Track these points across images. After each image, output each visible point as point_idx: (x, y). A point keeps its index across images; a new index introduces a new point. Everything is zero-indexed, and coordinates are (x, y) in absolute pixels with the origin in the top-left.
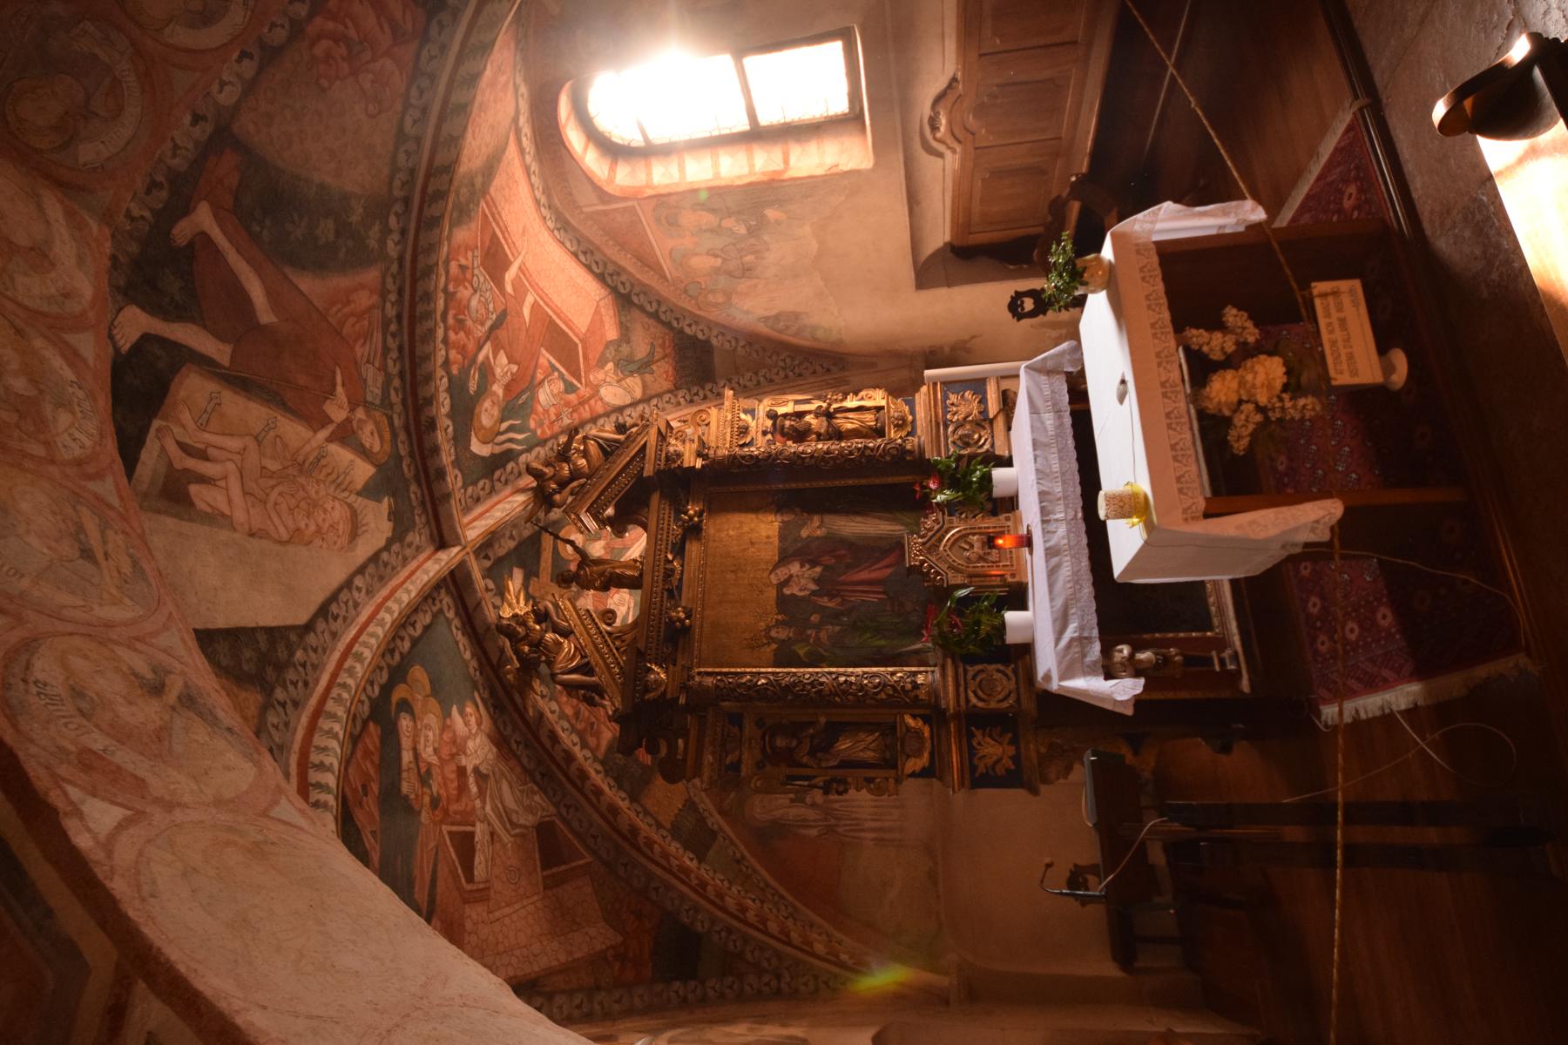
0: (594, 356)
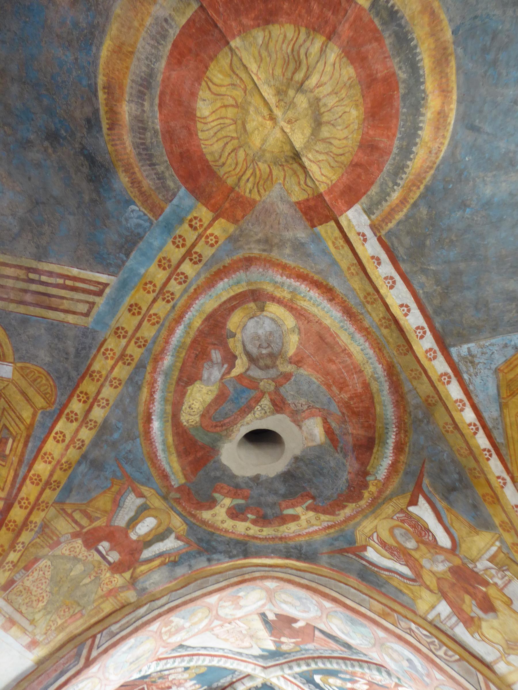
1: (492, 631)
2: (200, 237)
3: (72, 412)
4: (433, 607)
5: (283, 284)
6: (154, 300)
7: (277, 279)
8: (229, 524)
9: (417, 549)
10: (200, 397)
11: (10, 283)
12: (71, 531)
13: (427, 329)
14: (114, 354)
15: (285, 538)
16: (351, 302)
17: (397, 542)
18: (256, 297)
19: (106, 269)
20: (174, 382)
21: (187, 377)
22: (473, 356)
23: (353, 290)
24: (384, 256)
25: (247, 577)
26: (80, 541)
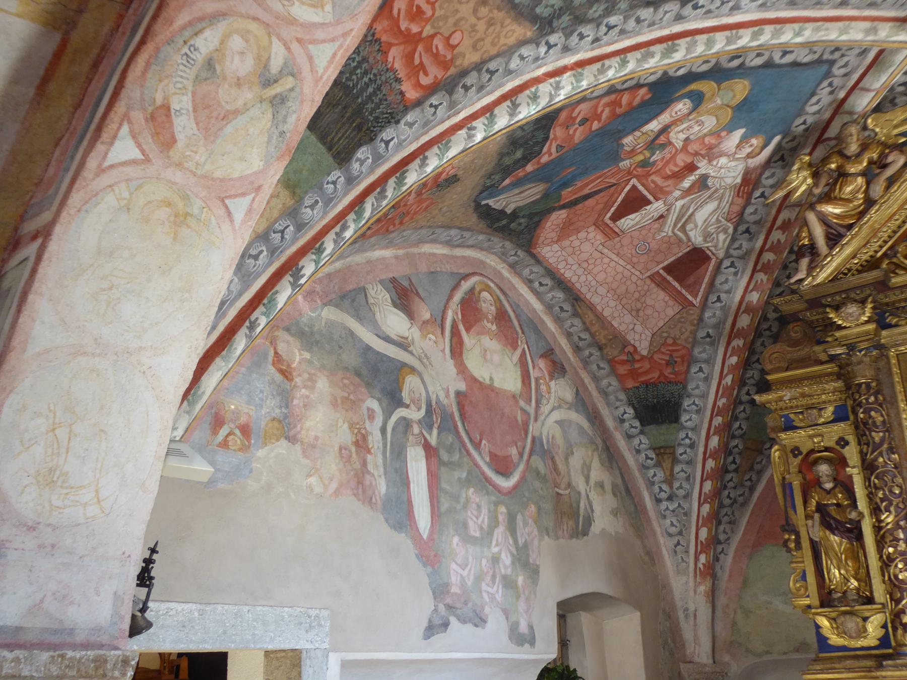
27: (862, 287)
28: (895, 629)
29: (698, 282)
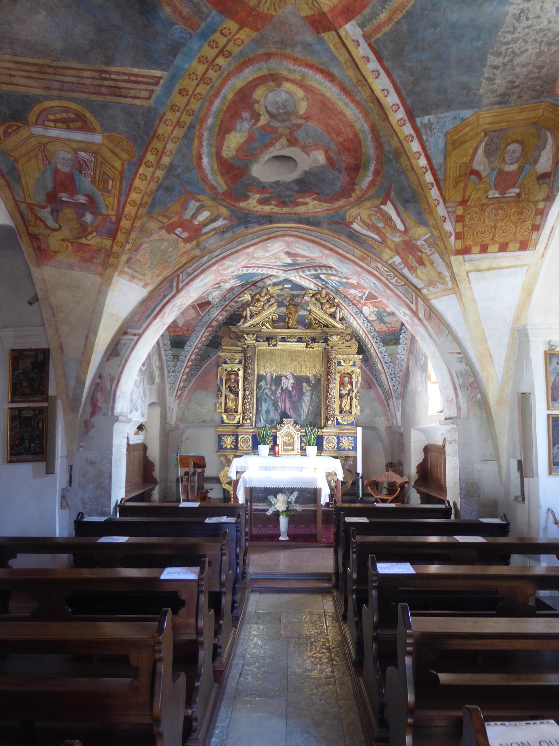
0: (377, 304)
1: (422, 274)
2: (229, 41)
3: (148, 161)
4: (392, 258)
5: (295, 71)
6: (198, 85)
7: (290, 68)
8: (259, 208)
9: (384, 228)
10: (234, 141)
11: (89, 81)
12: (158, 226)
13: (401, 106)
14: (172, 122)
15: (298, 213)
16: (347, 83)
17: (373, 223)
18: (275, 79)
19: (159, 67)
20: (216, 134)
21: (224, 129)
22: (431, 124)
23: (349, 76)
24: (372, 56)
25: (272, 235)
26: (164, 231)
27: (255, 331)
28: (243, 420)
29: (205, 310)
